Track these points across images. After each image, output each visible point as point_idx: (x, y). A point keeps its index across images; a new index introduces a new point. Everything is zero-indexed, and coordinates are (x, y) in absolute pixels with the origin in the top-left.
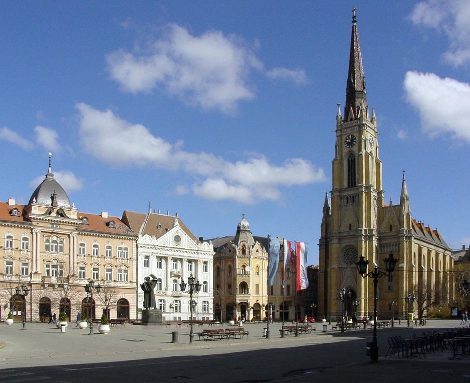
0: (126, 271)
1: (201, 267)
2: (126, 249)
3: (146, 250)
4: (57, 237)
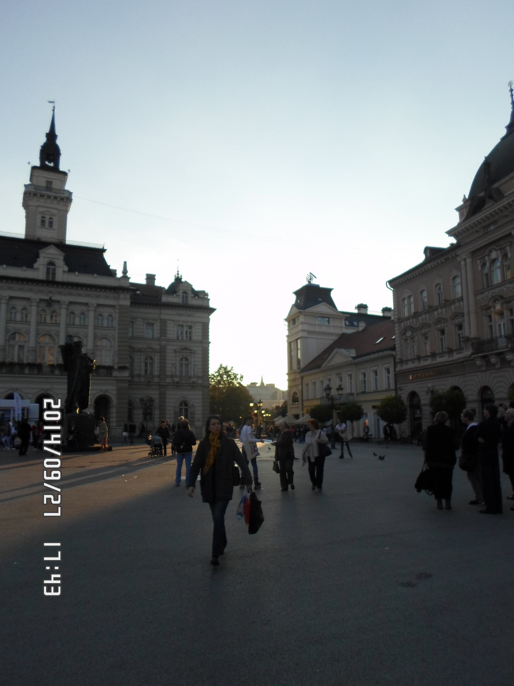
4: (495, 249)
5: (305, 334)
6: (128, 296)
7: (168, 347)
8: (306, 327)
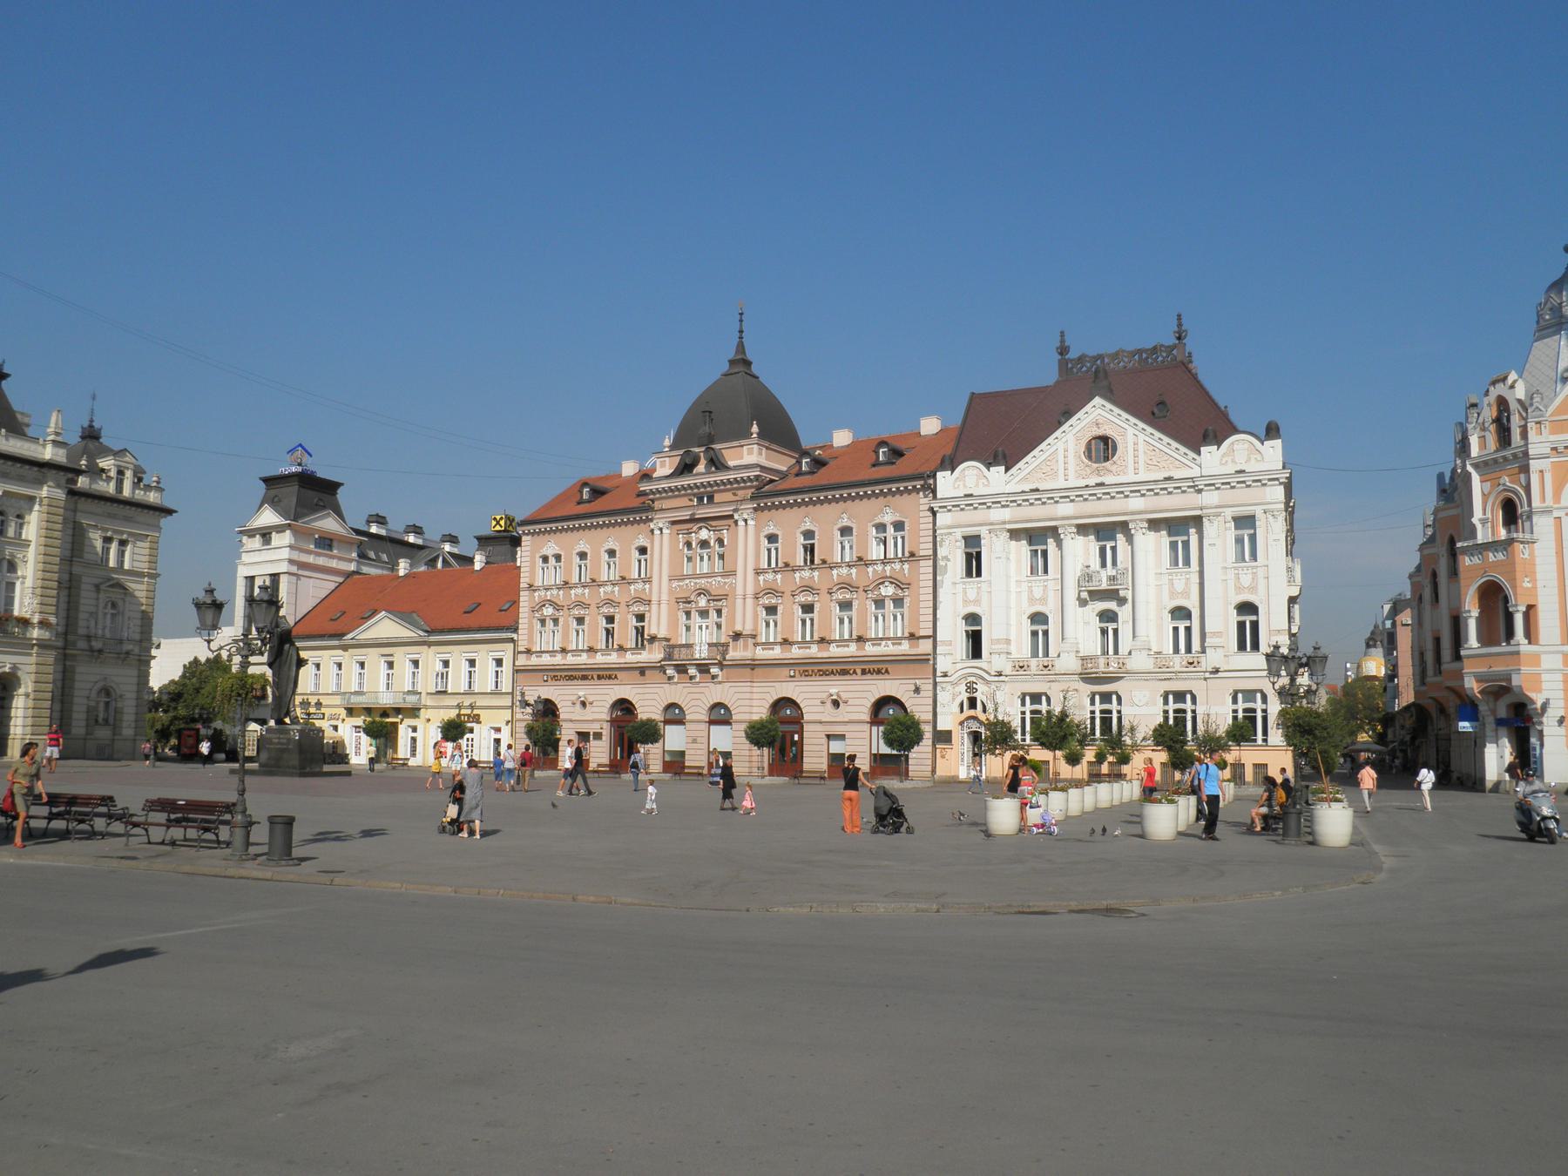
0: (898, 602)
1: (1219, 538)
2: (899, 526)
3: (969, 516)
5: (294, 569)
6: (63, 482)
7: (84, 579)
8: (296, 556)
